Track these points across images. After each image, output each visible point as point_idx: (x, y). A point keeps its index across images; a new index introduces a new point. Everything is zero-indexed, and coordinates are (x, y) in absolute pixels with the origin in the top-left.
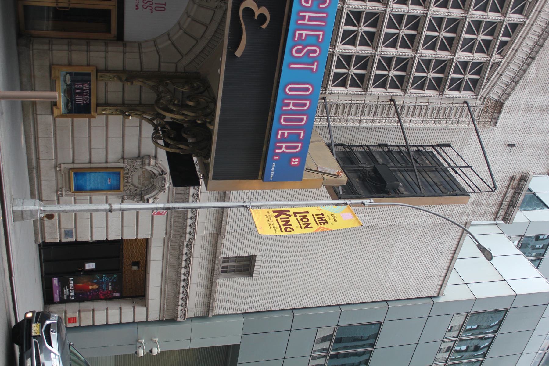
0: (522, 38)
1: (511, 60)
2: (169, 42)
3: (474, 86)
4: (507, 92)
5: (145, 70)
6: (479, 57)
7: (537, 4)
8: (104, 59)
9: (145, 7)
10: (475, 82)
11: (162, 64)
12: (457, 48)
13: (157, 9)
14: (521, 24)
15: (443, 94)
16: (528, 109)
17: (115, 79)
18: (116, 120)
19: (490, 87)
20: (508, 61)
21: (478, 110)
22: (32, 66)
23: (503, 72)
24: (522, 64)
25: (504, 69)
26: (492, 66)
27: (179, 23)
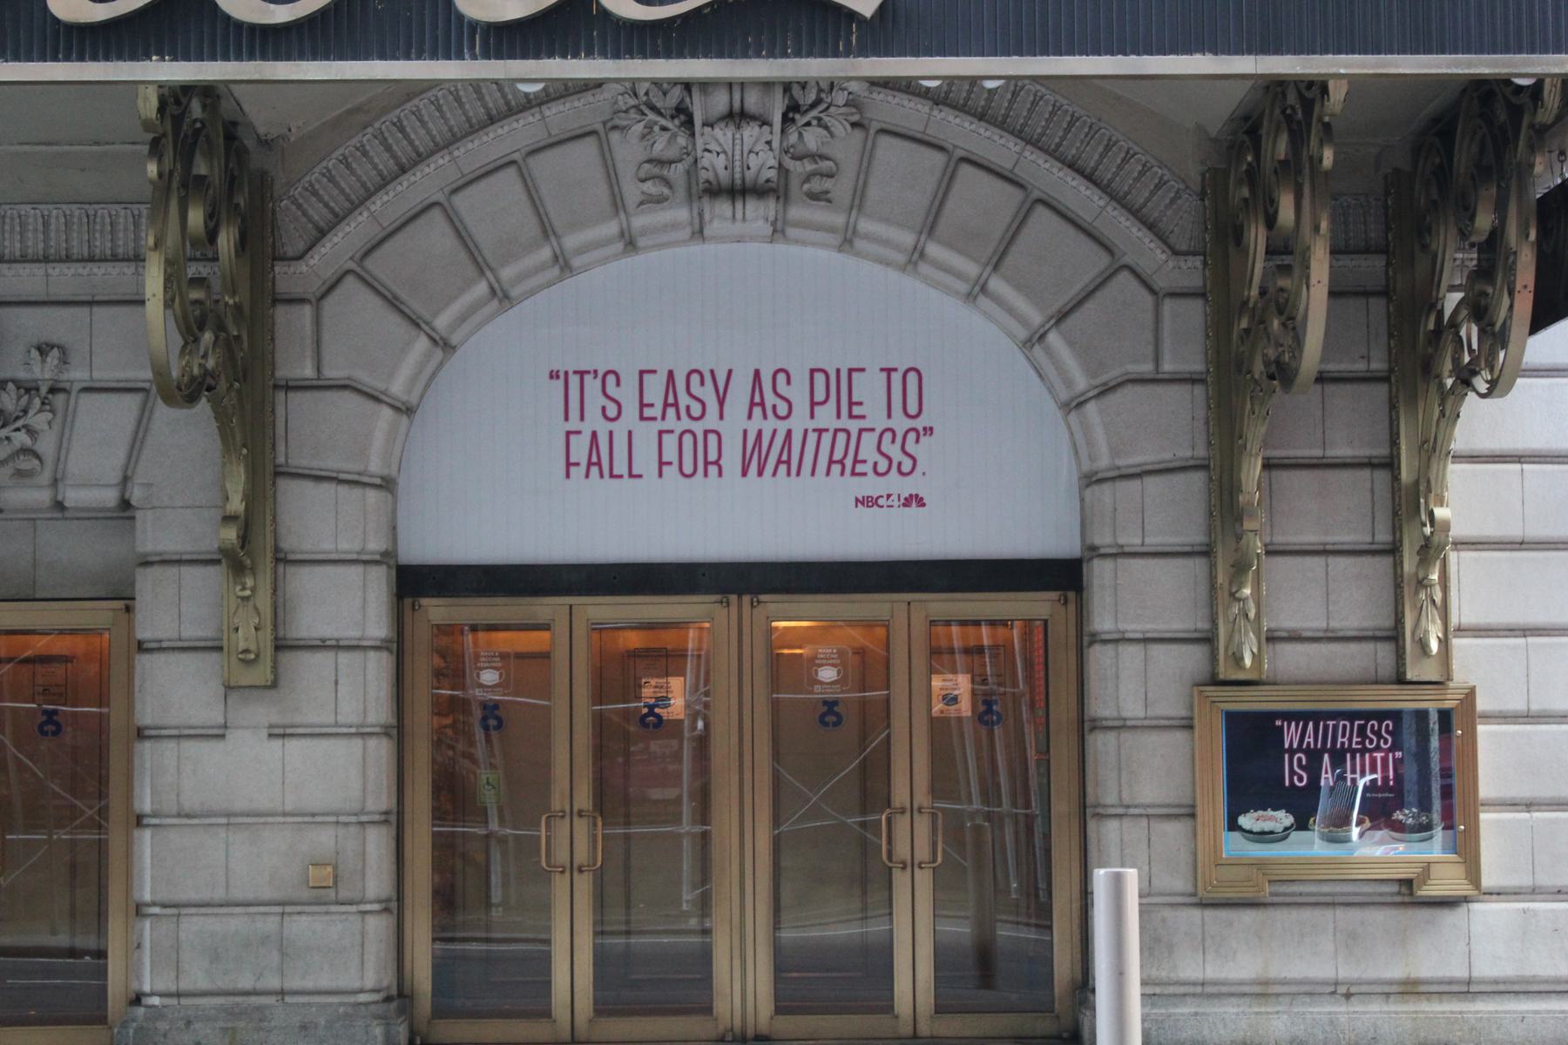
2: (1053, 338)
5: (1201, 452)
8: (1157, 650)
9: (907, 467)
11: (1168, 367)
13: (912, 410)
17: (1247, 591)
18: (1474, 588)
22: (1209, 989)
27: (970, 297)
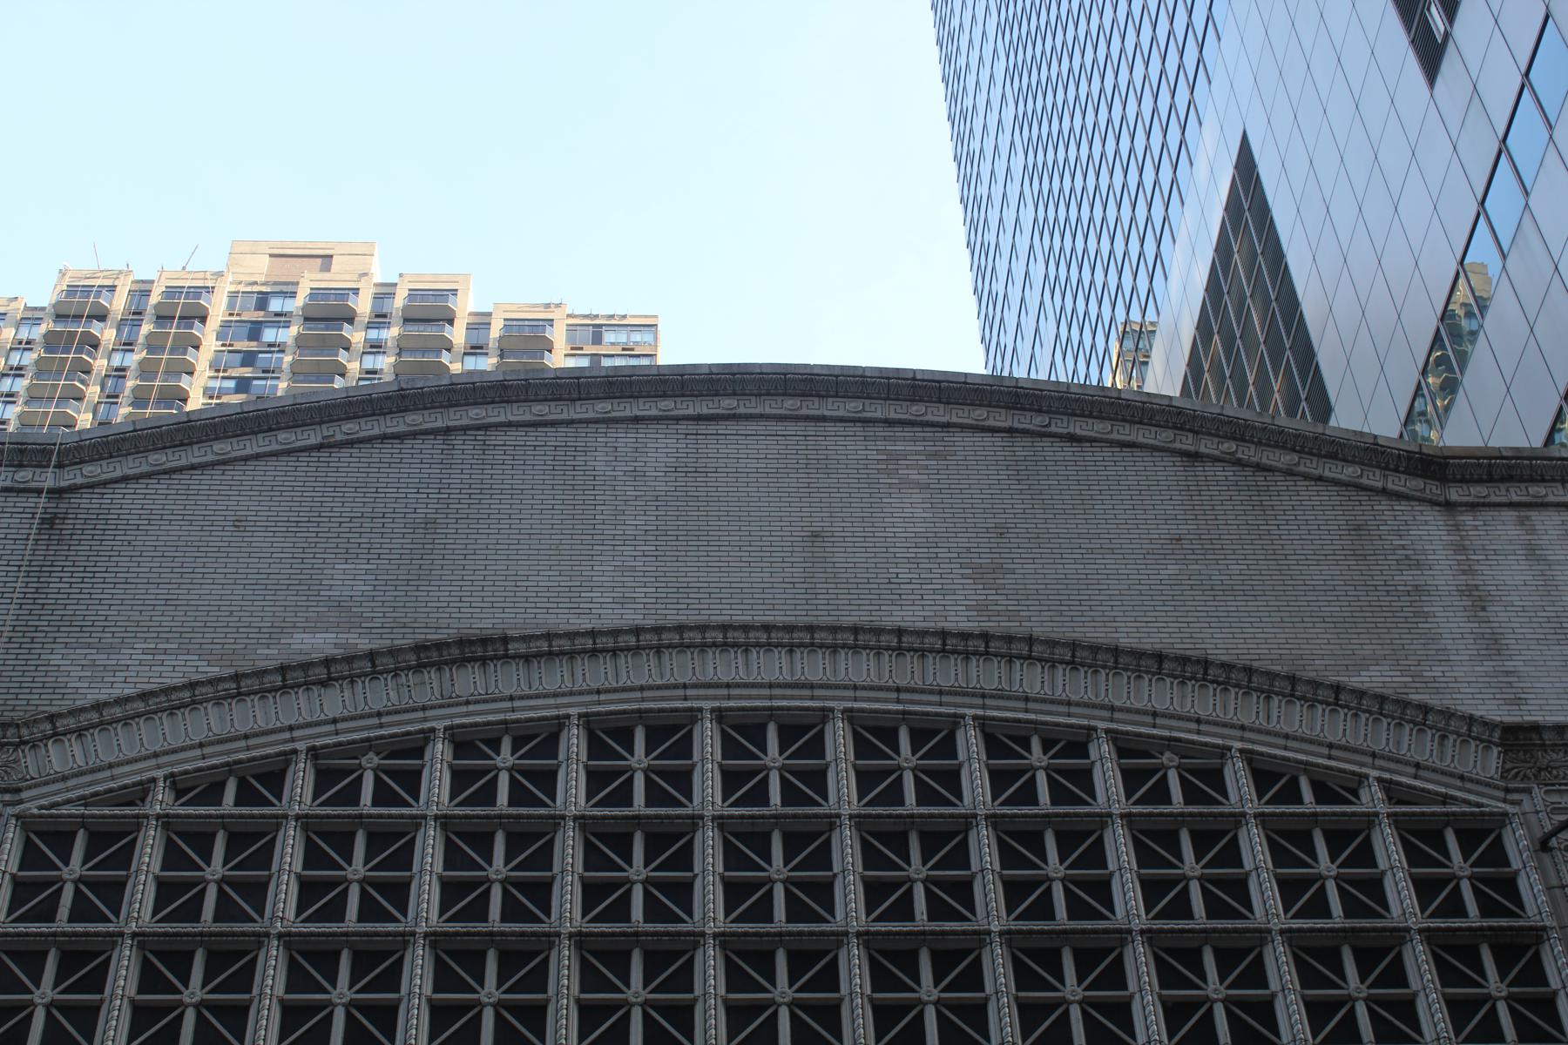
0: (1290, 744)
1: (1363, 753)
3: (1481, 835)
4: (1464, 730)
6: (1388, 850)
7: (1182, 735)
10: (1468, 840)
12: (1384, 930)
14: (1250, 762)
15: (1544, 929)
16: (1493, 645)
19: (1469, 785)
20: (1369, 760)
21: (1555, 798)
23: (1407, 763)
24: (1364, 716)
25: (1398, 761)
26: (1400, 802)
